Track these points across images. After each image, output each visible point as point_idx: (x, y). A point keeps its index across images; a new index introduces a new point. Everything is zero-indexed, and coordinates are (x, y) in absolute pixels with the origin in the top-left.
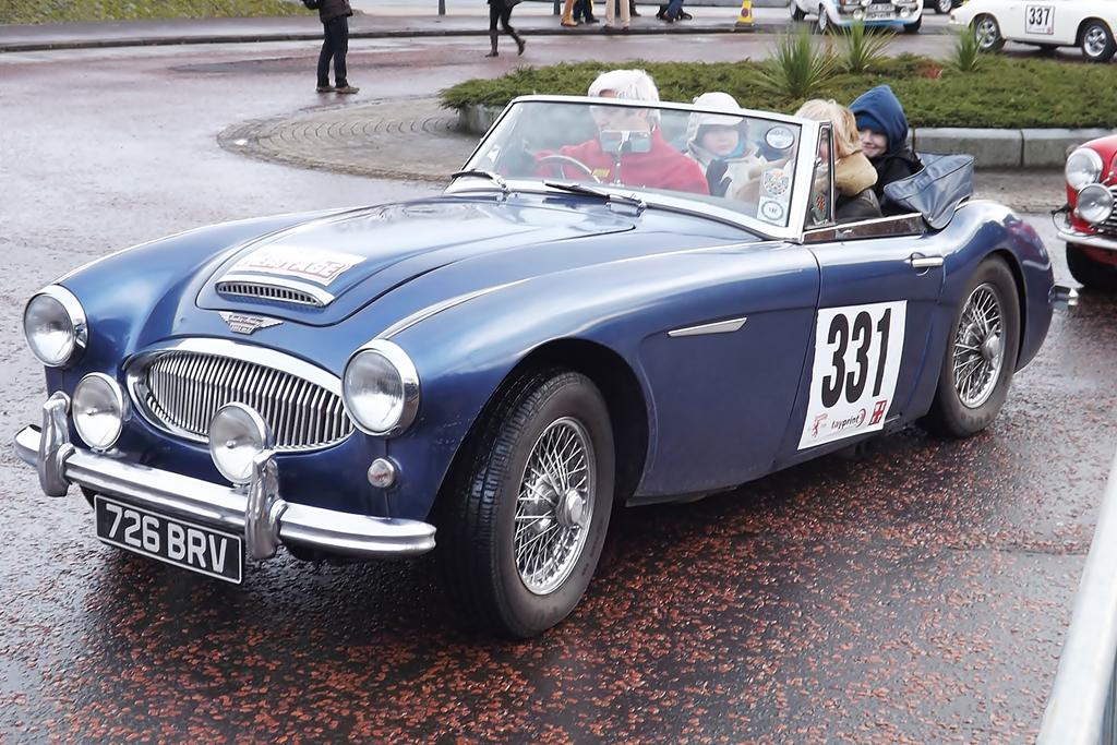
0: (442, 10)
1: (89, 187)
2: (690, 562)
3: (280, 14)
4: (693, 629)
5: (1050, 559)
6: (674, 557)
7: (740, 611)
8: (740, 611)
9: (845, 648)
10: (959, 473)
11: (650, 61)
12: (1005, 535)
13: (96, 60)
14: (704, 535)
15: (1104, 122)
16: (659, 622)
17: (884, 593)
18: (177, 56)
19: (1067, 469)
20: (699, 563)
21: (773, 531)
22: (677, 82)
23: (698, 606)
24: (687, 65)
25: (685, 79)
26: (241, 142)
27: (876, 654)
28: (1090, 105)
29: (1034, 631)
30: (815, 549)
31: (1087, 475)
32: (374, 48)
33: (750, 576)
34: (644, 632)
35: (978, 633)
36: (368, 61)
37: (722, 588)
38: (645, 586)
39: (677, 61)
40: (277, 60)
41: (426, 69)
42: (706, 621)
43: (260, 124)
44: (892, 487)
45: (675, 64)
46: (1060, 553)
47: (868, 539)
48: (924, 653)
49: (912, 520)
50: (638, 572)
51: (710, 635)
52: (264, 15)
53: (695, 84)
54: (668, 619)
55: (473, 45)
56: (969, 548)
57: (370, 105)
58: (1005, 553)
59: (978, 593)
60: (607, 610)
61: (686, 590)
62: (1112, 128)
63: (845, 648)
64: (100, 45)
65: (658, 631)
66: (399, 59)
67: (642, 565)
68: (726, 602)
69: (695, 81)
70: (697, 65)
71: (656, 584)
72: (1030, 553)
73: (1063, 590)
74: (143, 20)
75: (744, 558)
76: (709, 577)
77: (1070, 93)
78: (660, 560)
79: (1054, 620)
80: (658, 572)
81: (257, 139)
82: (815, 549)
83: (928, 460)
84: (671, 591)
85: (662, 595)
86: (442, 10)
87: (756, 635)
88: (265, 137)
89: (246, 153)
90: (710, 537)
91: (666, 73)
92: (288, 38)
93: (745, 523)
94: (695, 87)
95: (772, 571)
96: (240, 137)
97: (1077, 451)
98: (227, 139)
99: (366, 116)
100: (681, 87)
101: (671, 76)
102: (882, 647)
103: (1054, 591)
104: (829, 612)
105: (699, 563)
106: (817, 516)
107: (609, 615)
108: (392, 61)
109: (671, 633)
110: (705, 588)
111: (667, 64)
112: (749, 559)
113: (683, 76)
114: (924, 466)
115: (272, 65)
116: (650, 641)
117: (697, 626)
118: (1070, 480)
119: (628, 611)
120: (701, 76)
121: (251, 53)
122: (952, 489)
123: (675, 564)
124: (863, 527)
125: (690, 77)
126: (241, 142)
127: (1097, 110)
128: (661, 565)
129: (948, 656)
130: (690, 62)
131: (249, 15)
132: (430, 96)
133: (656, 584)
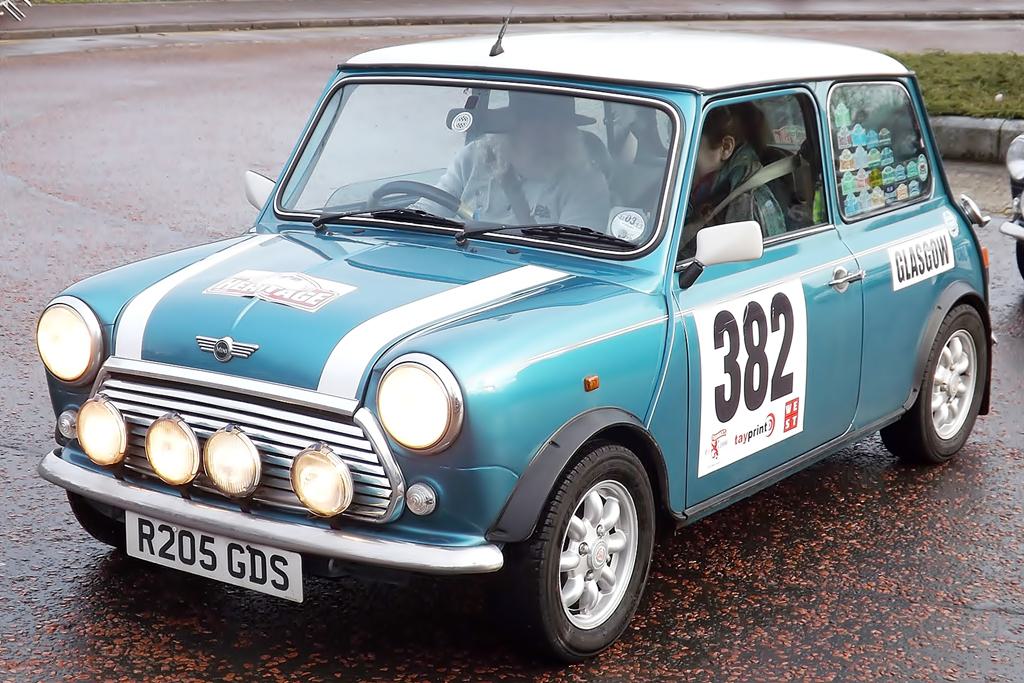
11: (951, 52)
13: (345, 40)
22: (978, 78)
24: (994, 57)
25: (990, 73)
39: (984, 52)
45: (981, 55)
50: (848, 639)
53: (1001, 79)
64: (351, 24)
67: (857, 633)
69: (1001, 75)
70: (1009, 58)
85: (872, 666)
91: (968, 65)
94: (1001, 82)
100: (983, 82)
101: (974, 70)
111: (971, 56)
113: (988, 70)
120: (1008, 69)
123: (895, 633)
125: (996, 70)
130: (999, 52)
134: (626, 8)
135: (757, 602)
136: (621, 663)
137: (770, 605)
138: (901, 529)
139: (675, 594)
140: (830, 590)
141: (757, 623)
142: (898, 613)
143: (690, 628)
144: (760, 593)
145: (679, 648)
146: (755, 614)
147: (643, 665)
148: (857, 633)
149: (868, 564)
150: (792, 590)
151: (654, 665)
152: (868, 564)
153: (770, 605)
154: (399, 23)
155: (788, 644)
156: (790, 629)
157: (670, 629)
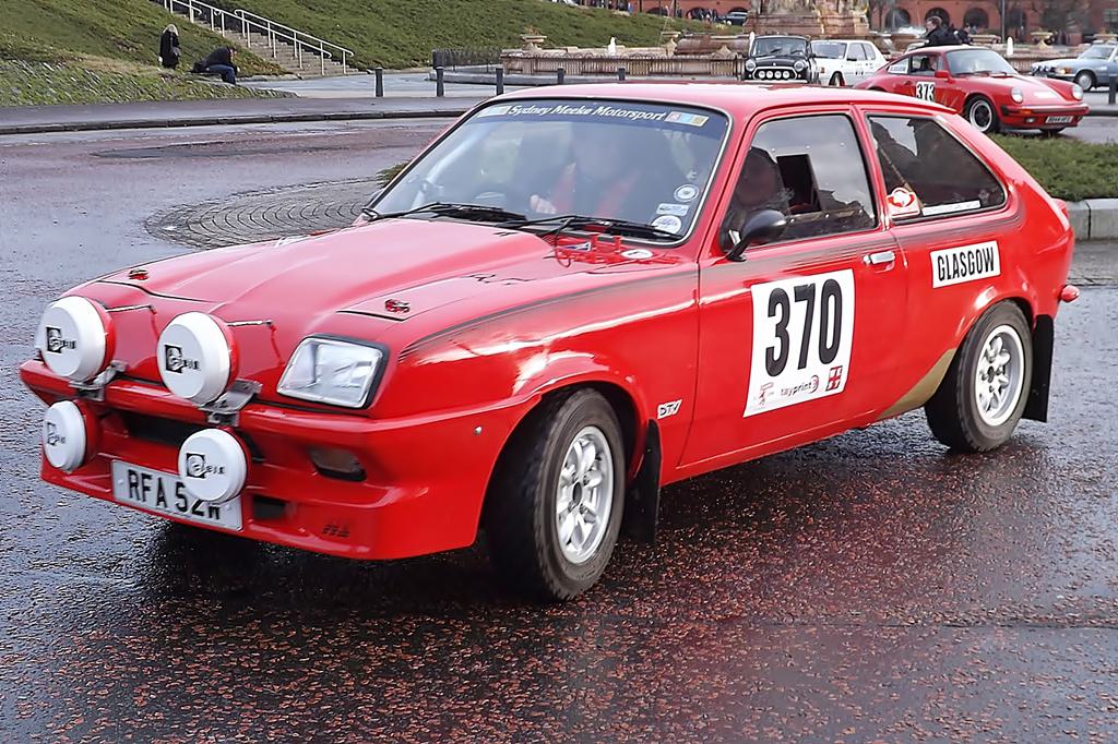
0: (379, 93)
1: (9, 275)
2: (674, 648)
3: (209, 98)
4: (682, 718)
5: (1053, 633)
6: (658, 644)
7: (732, 698)
8: (732, 698)
9: (848, 732)
10: (952, 549)
12: (1005, 611)
13: (14, 146)
14: (688, 619)
15: (1071, 195)
16: (646, 712)
17: (884, 674)
18: (99, 142)
19: (1062, 541)
20: (685, 650)
21: (761, 614)
23: (687, 694)
26: (170, 228)
27: (881, 738)
28: (1055, 178)
29: (1043, 707)
30: (807, 631)
31: (1084, 546)
32: (309, 131)
33: (739, 661)
34: (631, 724)
35: (985, 711)
36: (302, 144)
37: (711, 674)
38: (629, 676)
40: (205, 144)
41: (364, 152)
42: (696, 709)
43: (193, 209)
44: (884, 564)
46: (1063, 627)
47: (862, 620)
48: (930, 734)
49: (908, 598)
51: (702, 725)
52: (191, 99)
54: (655, 708)
55: (413, 128)
56: (969, 625)
57: (304, 189)
58: (1007, 628)
59: (982, 670)
60: (589, 700)
61: (673, 678)
62: (1079, 201)
63: (848, 732)
64: (18, 131)
65: (645, 722)
66: (334, 143)
67: (624, 654)
68: (717, 689)
71: (640, 673)
72: (1032, 628)
73: (1068, 663)
74: (63, 105)
75: (732, 643)
76: (701, 666)
77: (1035, 166)
78: (644, 647)
79: (1062, 694)
80: (641, 660)
81: (187, 224)
82: (807, 631)
83: (918, 535)
84: (657, 680)
85: (647, 683)
86: (379, 93)
87: (752, 722)
88: (196, 222)
89: (177, 238)
90: (695, 622)
92: (218, 122)
93: (730, 606)
95: (764, 654)
96: (169, 224)
97: (1070, 522)
98: (155, 225)
99: (301, 200)
102: (886, 731)
103: (1059, 665)
104: (827, 696)
105: (685, 650)
106: (807, 598)
107: (592, 705)
108: (326, 143)
109: (659, 722)
110: (694, 676)
112: (739, 645)
114: (916, 542)
115: (201, 149)
116: (637, 733)
117: (688, 715)
118: (1067, 552)
119: (612, 702)
121: (178, 138)
122: (946, 565)
123: (659, 651)
124: (856, 607)
126: (170, 228)
127: (1062, 183)
128: (643, 653)
129: (956, 736)
131: (175, 100)
132: (369, 179)
133: (640, 673)
134: (286, 110)
135: (525, 634)
136: (408, 701)
137: (538, 636)
138: (643, 559)
139: (444, 635)
140: (591, 618)
141: (530, 653)
142: (658, 633)
143: (468, 663)
144: (527, 626)
145: (460, 681)
146: (525, 645)
147: (429, 701)
148: (624, 654)
149: (621, 592)
150: (556, 621)
151: (440, 700)
152: (621, 592)
153: (538, 636)
154: (65, 129)
155: (563, 669)
156: (562, 655)
157: (447, 666)
